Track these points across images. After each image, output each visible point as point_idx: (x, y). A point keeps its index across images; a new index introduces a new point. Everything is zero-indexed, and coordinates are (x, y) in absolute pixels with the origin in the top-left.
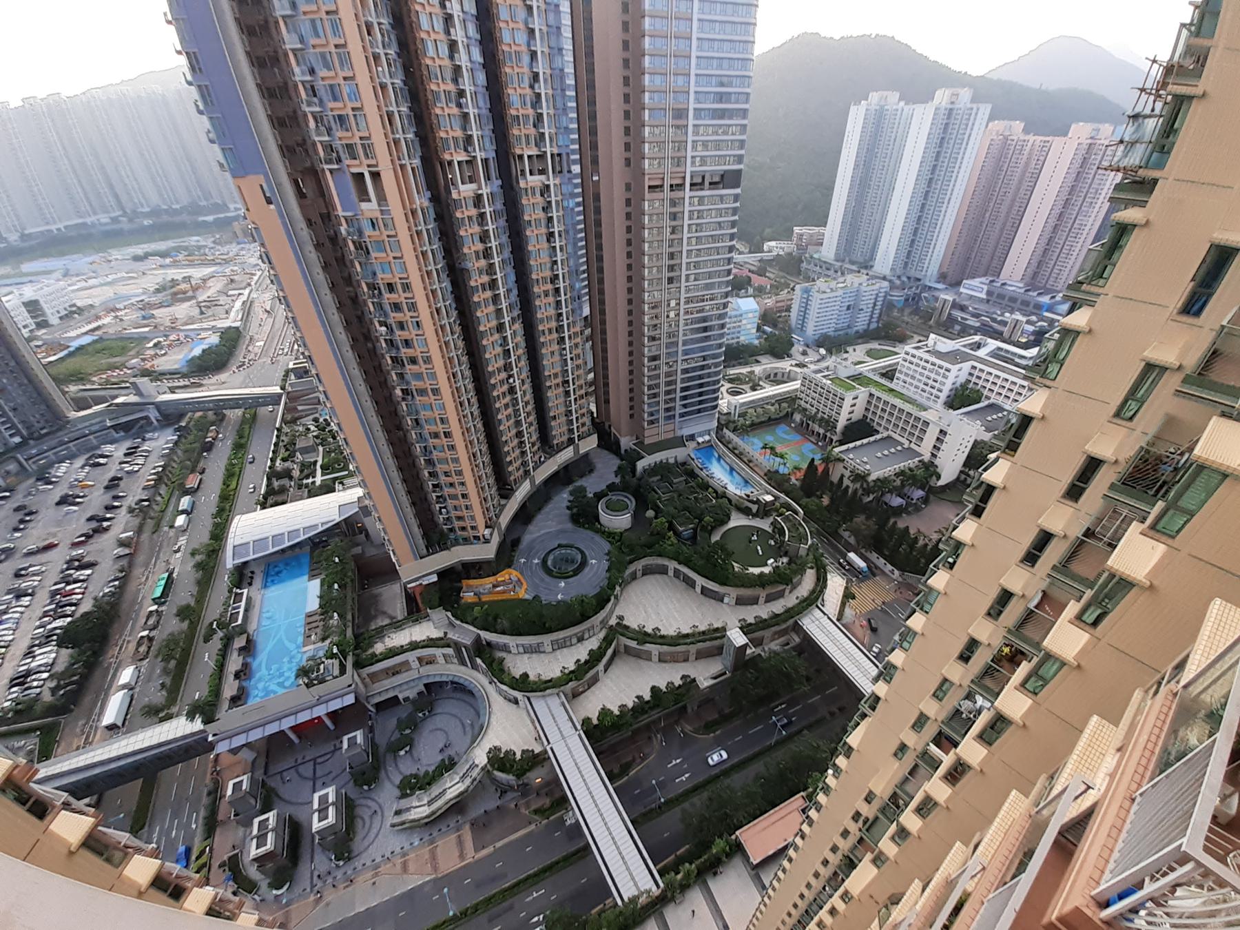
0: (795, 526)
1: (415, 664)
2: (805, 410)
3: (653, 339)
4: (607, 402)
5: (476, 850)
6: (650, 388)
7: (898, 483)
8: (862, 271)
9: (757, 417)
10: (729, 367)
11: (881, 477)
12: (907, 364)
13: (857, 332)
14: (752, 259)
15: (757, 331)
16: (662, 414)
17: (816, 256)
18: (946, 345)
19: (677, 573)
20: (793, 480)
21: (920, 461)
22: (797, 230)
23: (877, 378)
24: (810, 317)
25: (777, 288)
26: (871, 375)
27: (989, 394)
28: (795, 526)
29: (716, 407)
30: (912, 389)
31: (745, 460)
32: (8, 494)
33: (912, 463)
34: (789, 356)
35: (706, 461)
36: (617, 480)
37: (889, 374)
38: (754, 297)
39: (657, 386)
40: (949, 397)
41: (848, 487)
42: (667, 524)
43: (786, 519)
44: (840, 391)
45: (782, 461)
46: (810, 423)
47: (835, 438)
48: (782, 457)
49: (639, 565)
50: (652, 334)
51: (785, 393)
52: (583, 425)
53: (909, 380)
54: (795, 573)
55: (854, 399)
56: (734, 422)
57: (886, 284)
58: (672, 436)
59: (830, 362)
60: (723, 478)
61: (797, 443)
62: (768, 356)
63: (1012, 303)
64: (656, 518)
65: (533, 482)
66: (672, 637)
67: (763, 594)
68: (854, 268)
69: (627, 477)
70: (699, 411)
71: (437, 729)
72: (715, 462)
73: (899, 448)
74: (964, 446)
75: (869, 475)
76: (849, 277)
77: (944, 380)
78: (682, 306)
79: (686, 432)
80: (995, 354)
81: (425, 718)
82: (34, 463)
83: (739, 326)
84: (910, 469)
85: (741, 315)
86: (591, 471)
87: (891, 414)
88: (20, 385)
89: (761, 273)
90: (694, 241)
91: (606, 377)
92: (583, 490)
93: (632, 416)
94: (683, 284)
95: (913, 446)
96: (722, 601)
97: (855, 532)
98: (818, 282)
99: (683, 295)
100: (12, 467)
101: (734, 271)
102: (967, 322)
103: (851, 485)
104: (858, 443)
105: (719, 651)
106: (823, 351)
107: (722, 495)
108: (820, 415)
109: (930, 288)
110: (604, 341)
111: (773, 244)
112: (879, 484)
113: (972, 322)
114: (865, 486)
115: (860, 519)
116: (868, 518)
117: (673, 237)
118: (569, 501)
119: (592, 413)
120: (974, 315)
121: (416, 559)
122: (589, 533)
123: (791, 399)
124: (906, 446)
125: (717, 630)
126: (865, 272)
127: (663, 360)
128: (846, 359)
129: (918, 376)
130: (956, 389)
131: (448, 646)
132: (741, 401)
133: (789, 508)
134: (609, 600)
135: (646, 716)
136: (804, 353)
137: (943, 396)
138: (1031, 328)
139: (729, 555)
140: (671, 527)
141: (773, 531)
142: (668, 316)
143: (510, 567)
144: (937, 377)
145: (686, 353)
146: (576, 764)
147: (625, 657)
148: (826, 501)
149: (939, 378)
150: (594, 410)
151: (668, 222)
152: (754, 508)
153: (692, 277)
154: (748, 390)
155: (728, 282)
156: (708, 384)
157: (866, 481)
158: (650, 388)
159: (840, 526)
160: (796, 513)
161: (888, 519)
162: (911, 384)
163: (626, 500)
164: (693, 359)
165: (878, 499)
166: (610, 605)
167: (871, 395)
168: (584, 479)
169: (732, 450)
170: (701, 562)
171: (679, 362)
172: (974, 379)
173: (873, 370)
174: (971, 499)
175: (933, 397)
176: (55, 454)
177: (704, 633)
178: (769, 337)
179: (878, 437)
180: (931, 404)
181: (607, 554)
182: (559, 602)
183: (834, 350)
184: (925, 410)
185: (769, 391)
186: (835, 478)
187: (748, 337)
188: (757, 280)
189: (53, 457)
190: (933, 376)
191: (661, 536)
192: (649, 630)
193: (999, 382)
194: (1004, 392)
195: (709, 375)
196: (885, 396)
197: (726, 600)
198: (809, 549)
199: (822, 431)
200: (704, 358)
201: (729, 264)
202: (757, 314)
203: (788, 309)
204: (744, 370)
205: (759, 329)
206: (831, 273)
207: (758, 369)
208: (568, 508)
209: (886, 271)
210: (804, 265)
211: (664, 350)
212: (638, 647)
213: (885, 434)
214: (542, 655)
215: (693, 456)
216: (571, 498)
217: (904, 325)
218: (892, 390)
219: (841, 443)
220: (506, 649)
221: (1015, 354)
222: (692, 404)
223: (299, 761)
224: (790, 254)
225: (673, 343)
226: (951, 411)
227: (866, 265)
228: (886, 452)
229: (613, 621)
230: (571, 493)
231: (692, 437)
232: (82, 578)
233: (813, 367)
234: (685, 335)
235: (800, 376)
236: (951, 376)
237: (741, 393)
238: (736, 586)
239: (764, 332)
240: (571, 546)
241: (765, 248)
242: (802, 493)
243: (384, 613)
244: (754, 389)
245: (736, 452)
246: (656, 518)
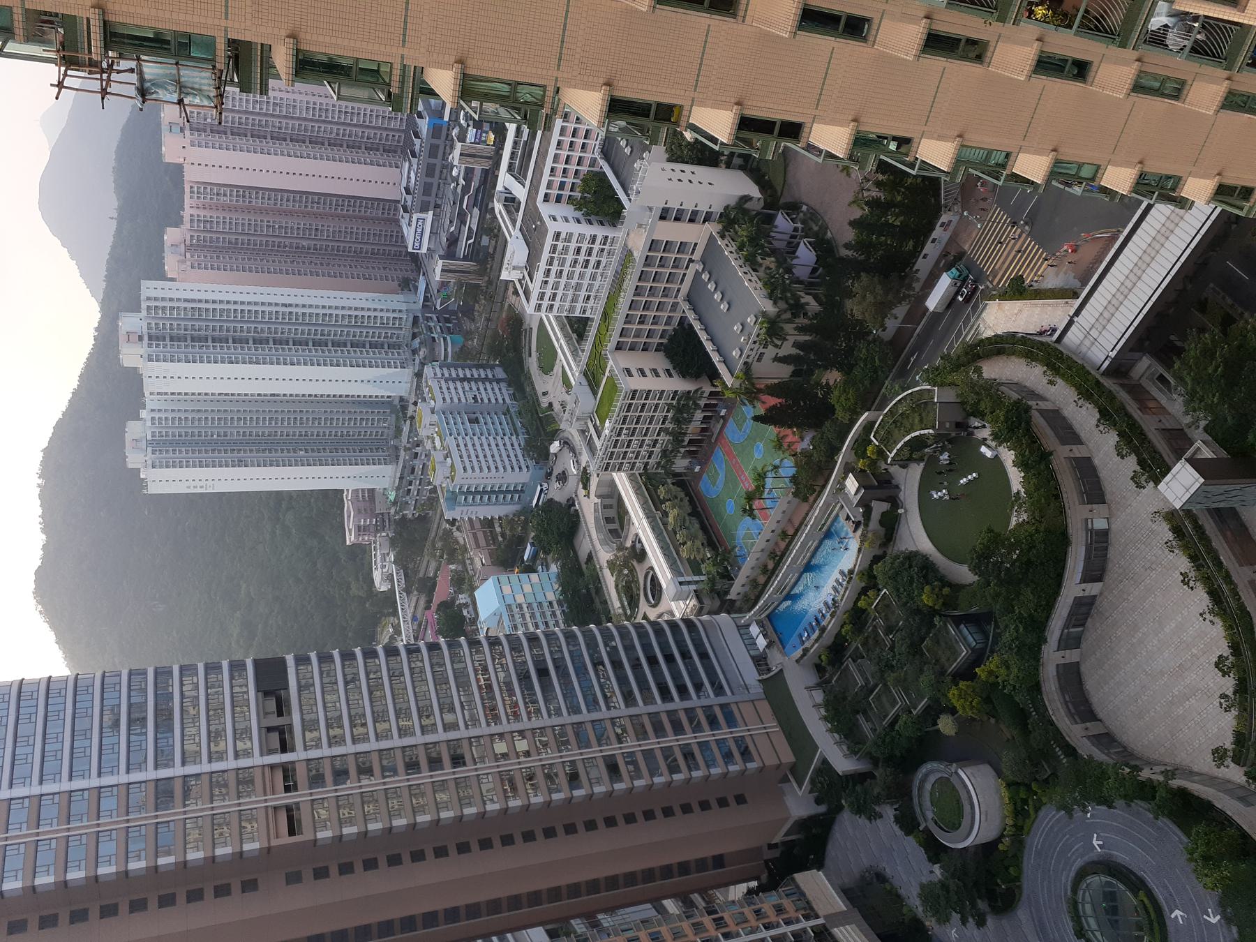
0: (898, 422)
2: (664, 453)
3: (574, 778)
4: (719, 861)
6: (674, 769)
7: (770, 262)
8: (410, 413)
9: (693, 538)
10: (606, 611)
11: (765, 292)
12: (557, 304)
13: (513, 397)
14: (406, 607)
15: (535, 571)
16: (724, 733)
17: (392, 498)
18: (516, 251)
19: (1070, 642)
20: (805, 445)
21: (723, 237)
22: (350, 539)
23: (588, 345)
24: (497, 482)
25: (453, 552)
26: (584, 357)
27: (587, 162)
28: (898, 422)
29: (688, 623)
30: (597, 284)
31: (783, 545)
33: (728, 249)
34: (571, 502)
35: (804, 623)
36: (889, 812)
37: (577, 327)
38: (472, 589)
39: (667, 752)
40: (602, 224)
41: (796, 345)
42: (962, 684)
43: (888, 441)
44: (620, 402)
45: (770, 474)
46: (687, 439)
47: (708, 389)
48: (761, 477)
49: (1075, 733)
50: (563, 780)
51: (637, 491)
52: (779, 910)
53: (583, 294)
54: (998, 400)
55: (630, 374)
56: (712, 581)
57: (428, 370)
58: (766, 703)
59: (572, 431)
60: (831, 582)
61: (729, 453)
62: (576, 543)
63: (435, 170)
64: (953, 711)
66: (1229, 628)
67: (1062, 454)
68: (406, 429)
69: (876, 791)
70: (704, 656)
72: (801, 605)
73: (705, 277)
74: (682, 176)
75: (764, 314)
76: (423, 432)
77: (575, 238)
78: (505, 727)
79: (751, 675)
80: (518, 172)
83: (530, 606)
84: (740, 248)
85: (509, 607)
86: (881, 877)
87: (647, 306)
89: (428, 587)
90: (381, 727)
91: (667, 871)
92: (928, 894)
94: (462, 733)
95: (697, 256)
96: (1104, 535)
97: (883, 309)
98: (437, 482)
99: (484, 729)
101: (430, 638)
102: (474, 227)
103: (791, 339)
104: (709, 347)
105: (1227, 518)
106: (555, 447)
107: (867, 578)
108: (670, 426)
109: (426, 299)
110: (594, 886)
111: (377, 576)
112: (778, 293)
113: (473, 221)
114: (788, 315)
115: (854, 308)
116: (850, 295)
117: (377, 769)
118: (964, 921)
119: (750, 892)
120: (463, 222)
122: (1029, 861)
123: (648, 484)
124: (700, 267)
125: (1178, 531)
126: (411, 408)
127: (613, 749)
128: (563, 405)
129: (574, 282)
130: (584, 215)
132: (669, 575)
133: (861, 444)
134: (1183, 794)
136: (563, 477)
137: (600, 232)
138: (471, 132)
139: (996, 539)
140: (967, 673)
141: (921, 459)
142: (527, 754)
144: (571, 251)
145: (592, 704)
148: (833, 377)
149: (573, 245)
150: (741, 889)
151: (350, 787)
152: (879, 508)
153: (449, 718)
154: (646, 565)
155: (450, 646)
156: (647, 647)
157: (778, 315)
158: (674, 769)
159: (877, 340)
160: (868, 427)
161: (842, 260)
162: (590, 287)
163: (928, 786)
164: (602, 687)
165: (809, 287)
166: (1195, 788)
167: (619, 347)
168: (902, 892)
169: (770, 573)
170: (1028, 594)
171: (614, 713)
172: (566, 193)
173: (575, 353)
174: (769, 148)
175: (607, 247)
177: (1193, 558)
178: (543, 547)
179: (691, 316)
180: (618, 247)
181: (1069, 812)
182: (1227, 919)
183: (549, 429)
184: (630, 253)
185: (640, 525)
186: (785, 371)
187: (547, 586)
188: (443, 590)
190: (570, 257)
191: (991, 696)
192: (1228, 684)
193: (564, 153)
194: (579, 141)
195: (629, 648)
196: (618, 324)
198: (941, 385)
199: (699, 415)
200: (597, 663)
201: (418, 650)
202: (504, 578)
203: (488, 523)
204: (609, 580)
205: (530, 569)
206: (418, 465)
207: (604, 555)
208: (981, 923)
209: (406, 375)
210: (409, 513)
211: (595, 752)
213: (685, 306)
215: (799, 652)
216: (956, 917)
217: (492, 326)
218: (606, 316)
219: (714, 375)
221: (515, 143)
222: (693, 673)
224: (393, 543)
225: (577, 735)
226: (625, 213)
227: (400, 409)
228: (717, 296)
229: (1235, 773)
230: (944, 920)
231: (760, 661)
233: (585, 458)
234: (558, 712)
235: (605, 476)
236: (564, 228)
237: (655, 583)
238: (1061, 511)
239: (534, 557)
240: (1074, 906)
241: (384, 588)
242: (828, 424)
244: (641, 555)
245: (771, 566)
246: (953, 711)
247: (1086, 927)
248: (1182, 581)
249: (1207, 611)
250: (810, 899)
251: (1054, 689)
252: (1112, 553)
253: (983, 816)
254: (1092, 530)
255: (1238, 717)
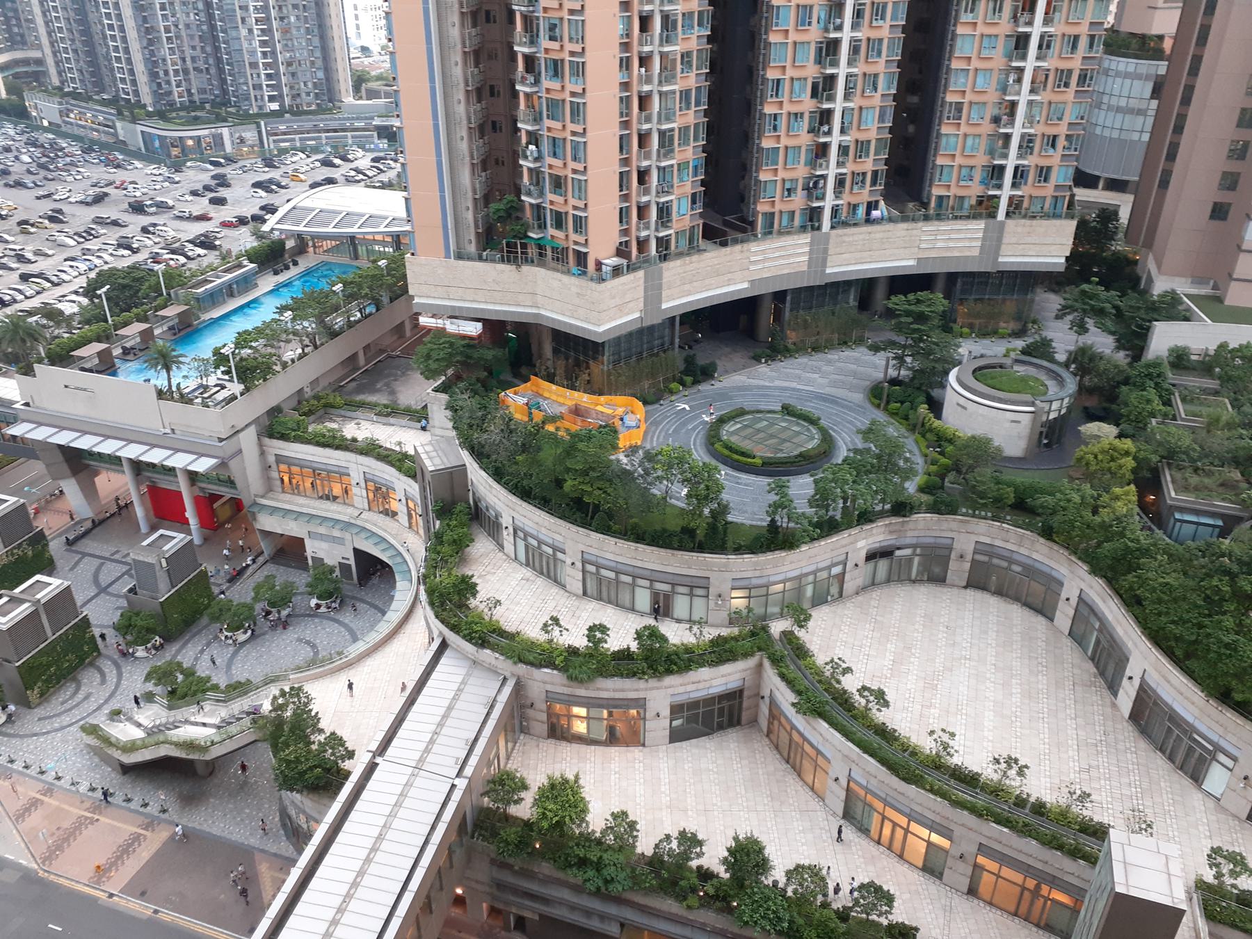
1: (359, 495)
5: (128, 890)
32: (222, 161)
65: (819, 256)
71: (308, 643)
81: (314, 613)
82: (274, 141)
88: (308, 31)
93: (1219, 212)
100: (250, 135)
121: (448, 256)
131: (413, 476)
135: (669, 905)
143: (646, 403)
146: (380, 838)
147: (762, 746)
176: (301, 139)
177: (1040, 808)
189: (298, 144)
192: (850, 684)
197: (1217, 778)
212: (790, 712)
214: (555, 590)
220: (493, 528)
223: (117, 557)
232: (190, 254)
243: (393, 393)
247: (787, 417)
248: (1016, 761)
249: (951, 743)
250: (1035, 222)
251: (1035, 556)
252: (1159, 762)
253: (962, 401)
254: (1214, 759)
255: (819, 673)
